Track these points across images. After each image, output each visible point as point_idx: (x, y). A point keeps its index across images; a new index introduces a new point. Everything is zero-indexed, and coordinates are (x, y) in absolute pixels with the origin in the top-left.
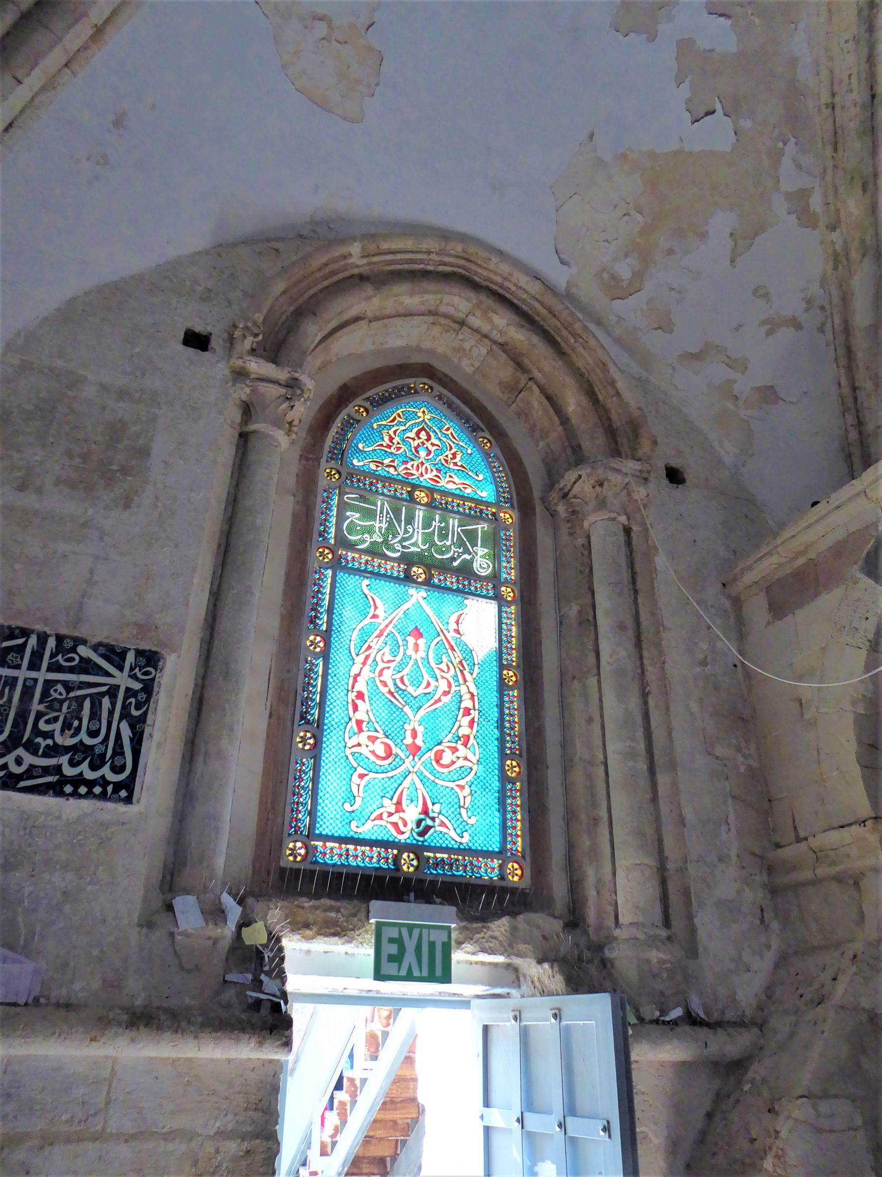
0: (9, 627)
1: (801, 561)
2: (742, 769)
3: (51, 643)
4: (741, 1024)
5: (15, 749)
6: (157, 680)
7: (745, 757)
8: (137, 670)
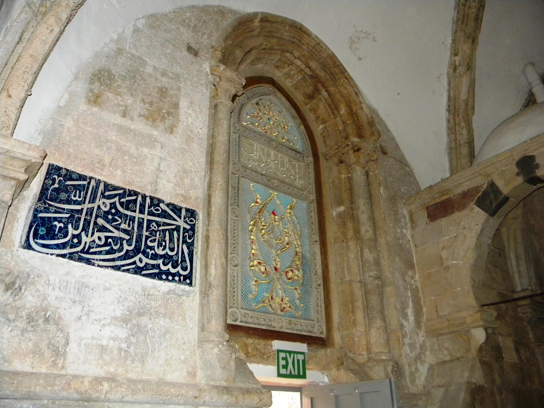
0: (129, 190)
1: (444, 198)
2: (414, 287)
3: (148, 201)
5: (138, 254)
6: (196, 225)
7: (415, 281)
8: (187, 219)
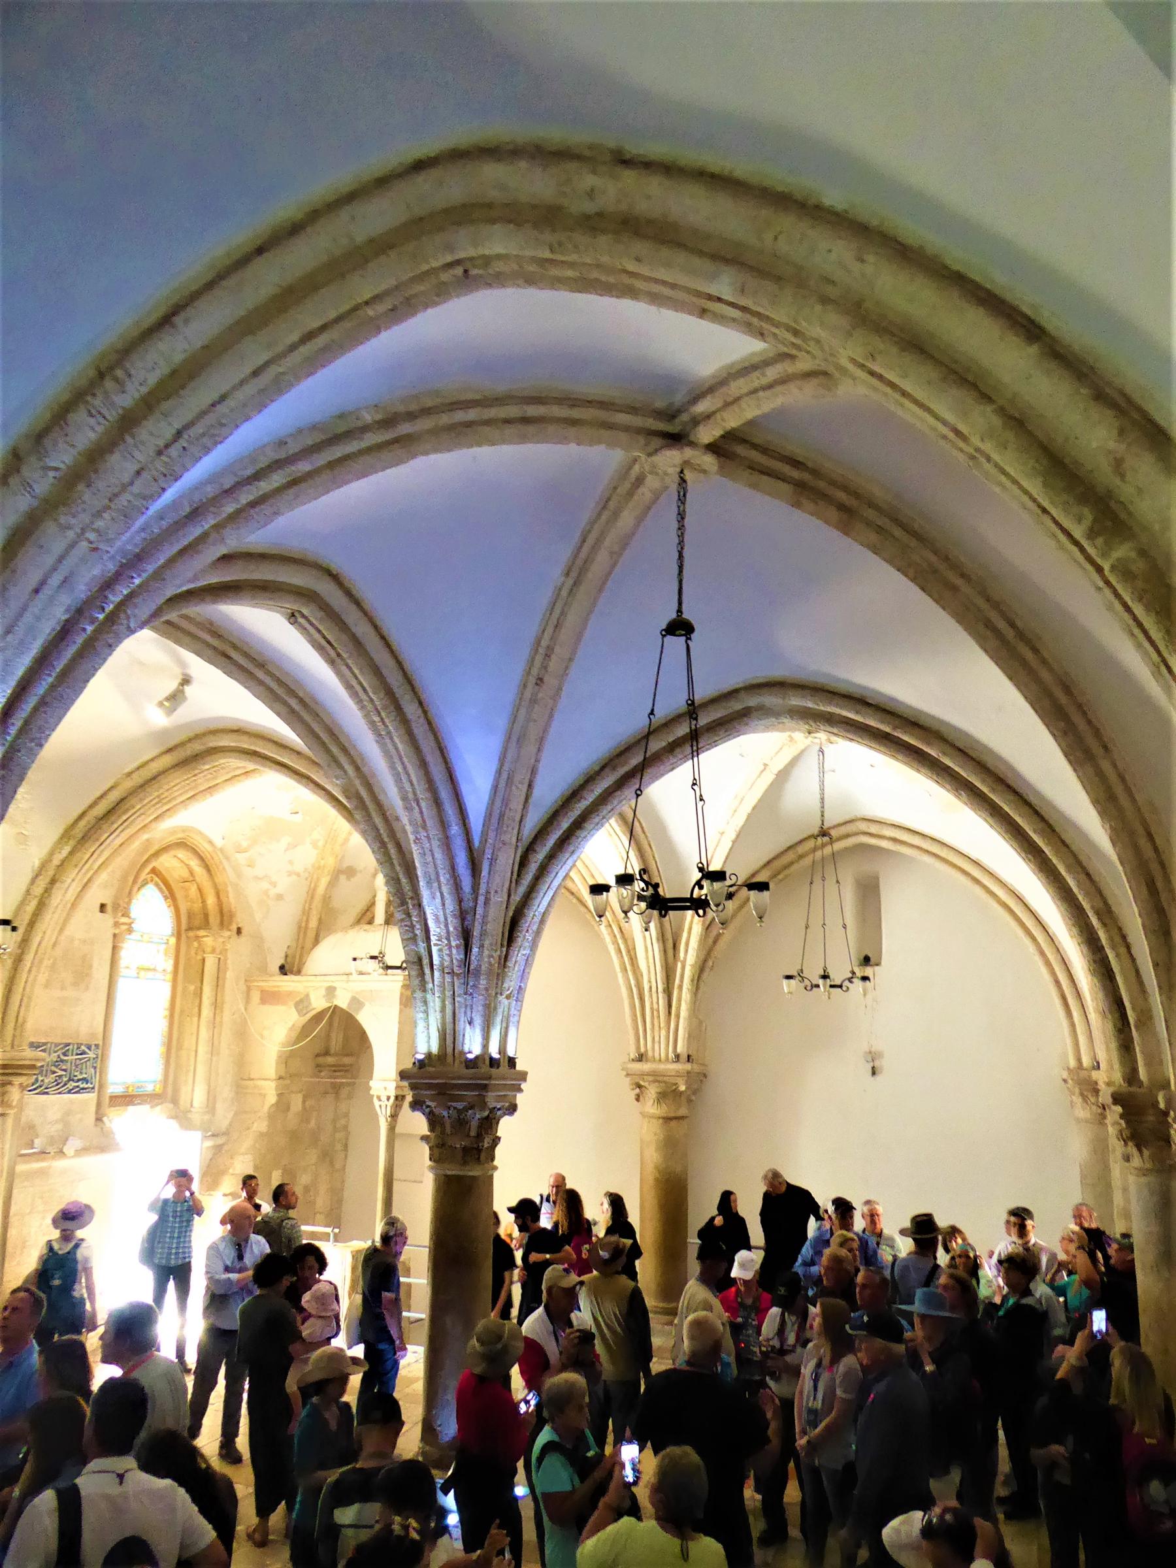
4: (224, 1134)
